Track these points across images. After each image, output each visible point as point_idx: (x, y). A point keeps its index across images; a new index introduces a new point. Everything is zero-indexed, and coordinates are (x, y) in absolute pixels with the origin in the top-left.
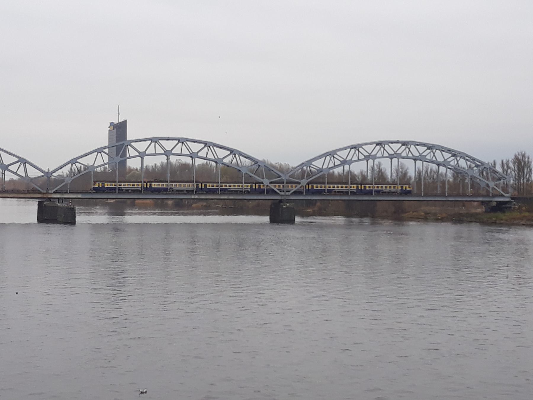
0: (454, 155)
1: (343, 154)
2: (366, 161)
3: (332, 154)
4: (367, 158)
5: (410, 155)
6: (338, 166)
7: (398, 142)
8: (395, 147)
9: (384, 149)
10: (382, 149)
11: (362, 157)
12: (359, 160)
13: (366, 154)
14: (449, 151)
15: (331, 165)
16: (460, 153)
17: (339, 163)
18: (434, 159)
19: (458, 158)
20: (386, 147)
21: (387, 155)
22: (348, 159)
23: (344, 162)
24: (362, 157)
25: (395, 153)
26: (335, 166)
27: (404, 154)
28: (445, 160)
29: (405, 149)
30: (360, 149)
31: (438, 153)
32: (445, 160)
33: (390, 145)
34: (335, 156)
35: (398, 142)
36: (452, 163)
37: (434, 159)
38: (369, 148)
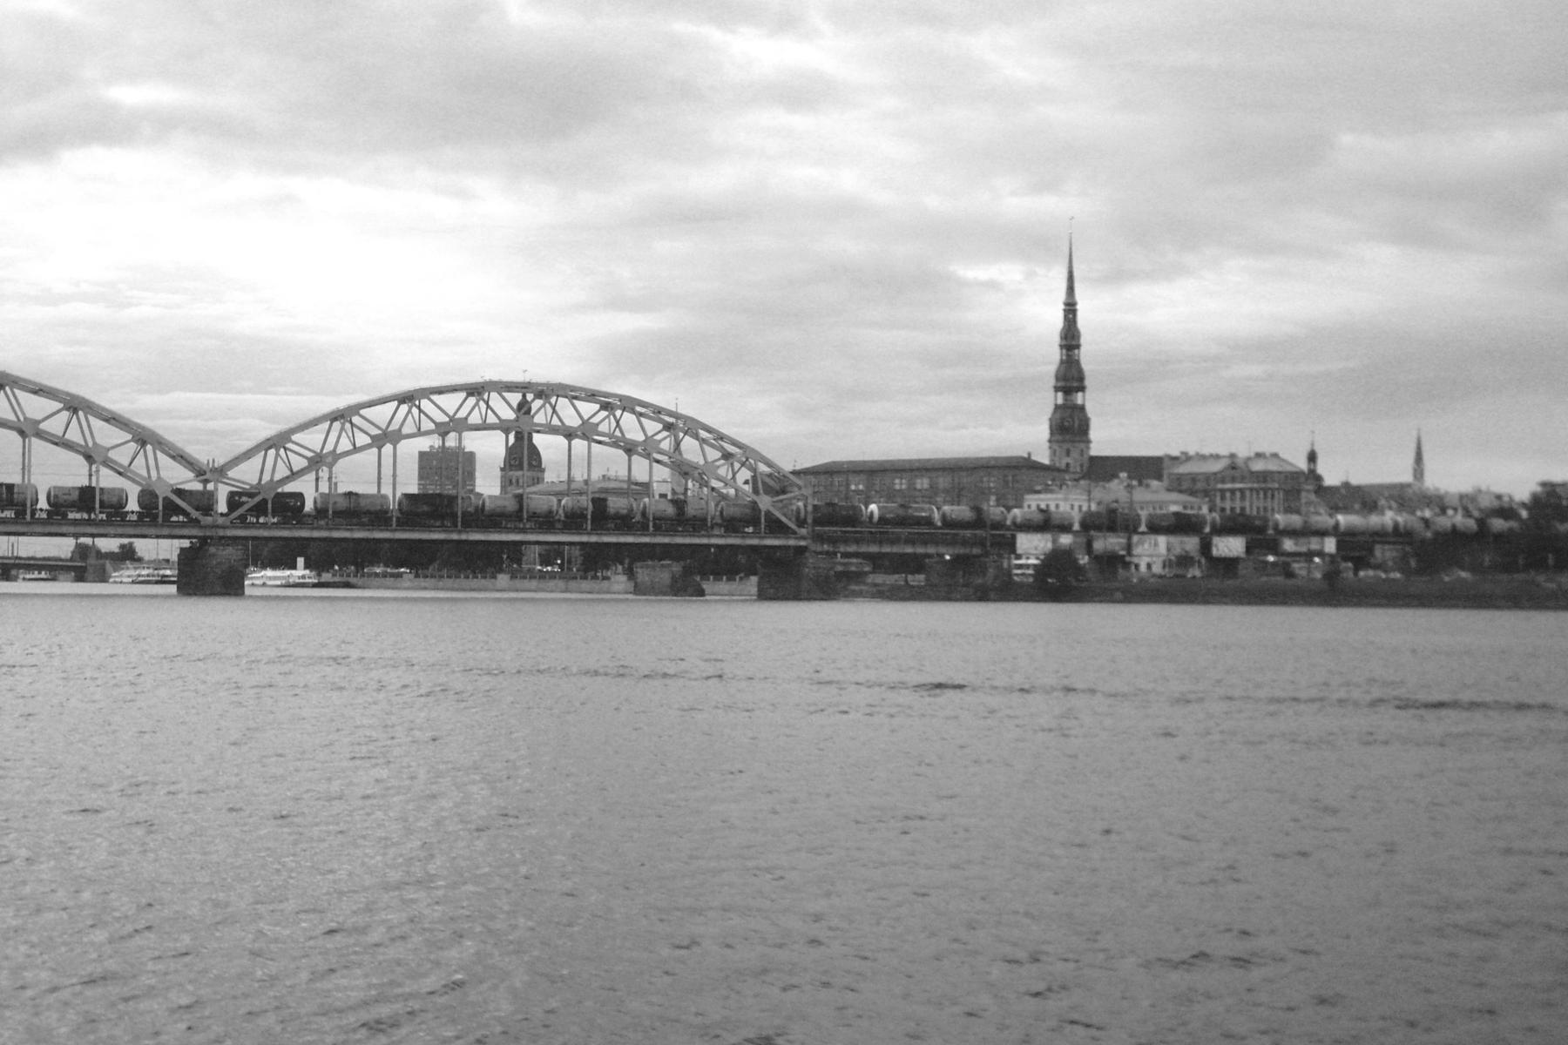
0: (605, 406)
1: (312, 439)
2: (375, 450)
3: (278, 442)
4: (379, 441)
5: (492, 419)
6: (302, 472)
7: (453, 389)
8: (450, 402)
9: (420, 411)
10: (415, 411)
11: (361, 439)
12: (356, 449)
13: (375, 432)
14: (591, 396)
15: (283, 471)
16: (621, 398)
17: (304, 463)
18: (555, 422)
19: (618, 413)
20: (425, 404)
21: (432, 426)
22: (329, 447)
23: (317, 461)
24: (361, 439)
25: (452, 419)
26: (294, 475)
27: (475, 419)
28: (585, 422)
29: (477, 404)
30: (356, 420)
31: (563, 404)
32: (585, 422)
33: (434, 397)
34: (289, 445)
35: (453, 389)
36: (603, 428)
37: (618, 433)
38: (381, 414)
